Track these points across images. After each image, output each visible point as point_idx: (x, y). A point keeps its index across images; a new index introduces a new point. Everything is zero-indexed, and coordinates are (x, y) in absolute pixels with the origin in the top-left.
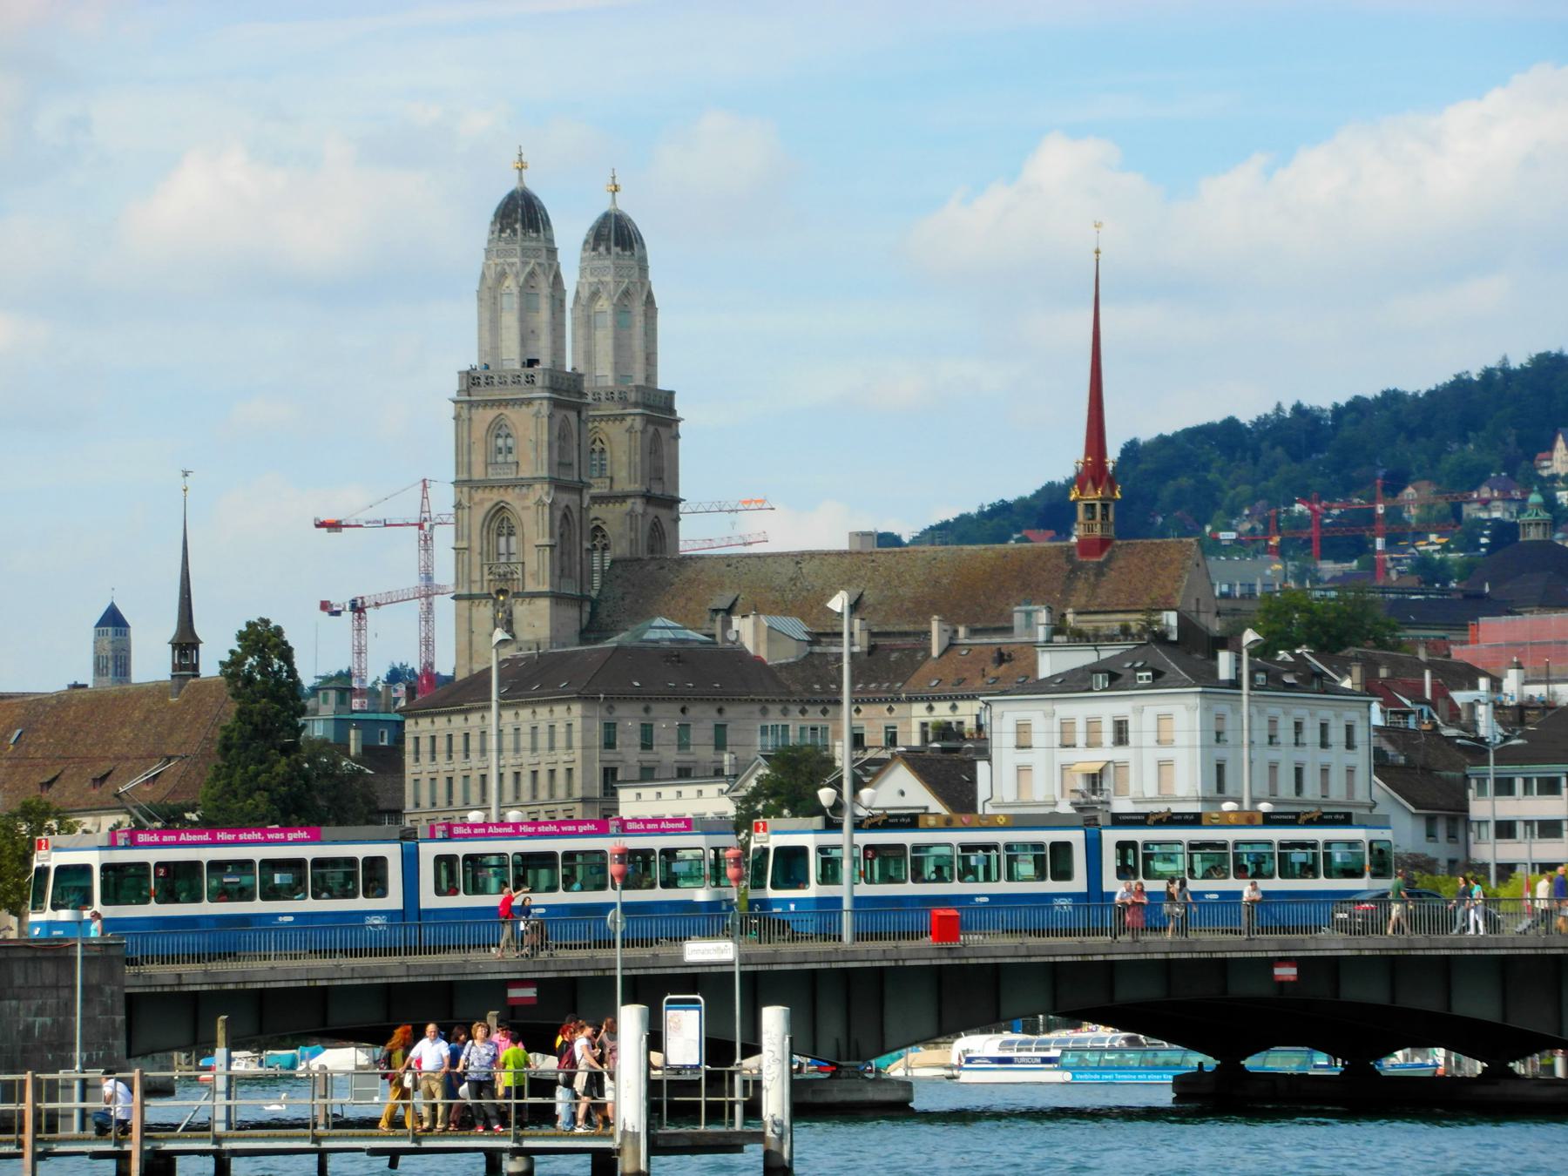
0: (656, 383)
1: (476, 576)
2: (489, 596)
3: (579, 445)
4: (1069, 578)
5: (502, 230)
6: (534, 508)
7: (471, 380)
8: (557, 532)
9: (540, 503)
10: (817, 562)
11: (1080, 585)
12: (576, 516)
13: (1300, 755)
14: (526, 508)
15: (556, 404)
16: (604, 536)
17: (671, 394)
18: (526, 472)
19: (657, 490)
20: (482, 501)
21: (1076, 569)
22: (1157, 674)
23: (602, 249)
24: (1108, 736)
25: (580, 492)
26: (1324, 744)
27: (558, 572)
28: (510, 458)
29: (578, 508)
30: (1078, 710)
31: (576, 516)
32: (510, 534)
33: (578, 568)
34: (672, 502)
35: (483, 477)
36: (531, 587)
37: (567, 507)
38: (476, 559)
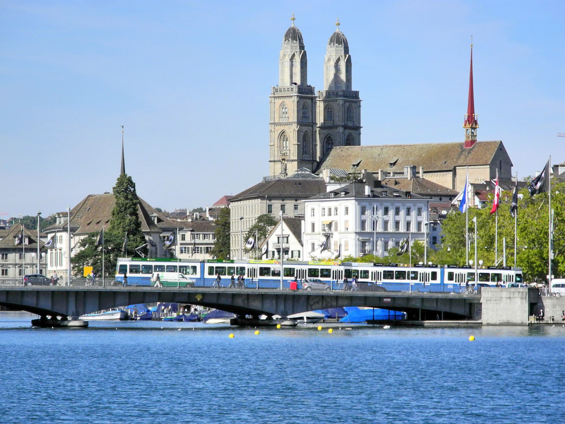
0: (351, 89)
1: (276, 154)
2: (279, 161)
3: (312, 111)
4: (460, 154)
5: (285, 41)
6: (293, 132)
8: (301, 139)
9: (294, 130)
10: (387, 149)
11: (463, 157)
14: (290, 132)
15: (300, 98)
16: (332, 140)
18: (291, 120)
19: (350, 124)
20: (278, 130)
21: (463, 150)
23: (332, 44)
25: (312, 126)
27: (302, 153)
28: (287, 115)
29: (311, 132)
30: (327, 204)
31: (310, 135)
32: (287, 140)
33: (311, 151)
34: (358, 128)
35: (278, 122)
36: (292, 158)
37: (306, 131)
38: (276, 149)
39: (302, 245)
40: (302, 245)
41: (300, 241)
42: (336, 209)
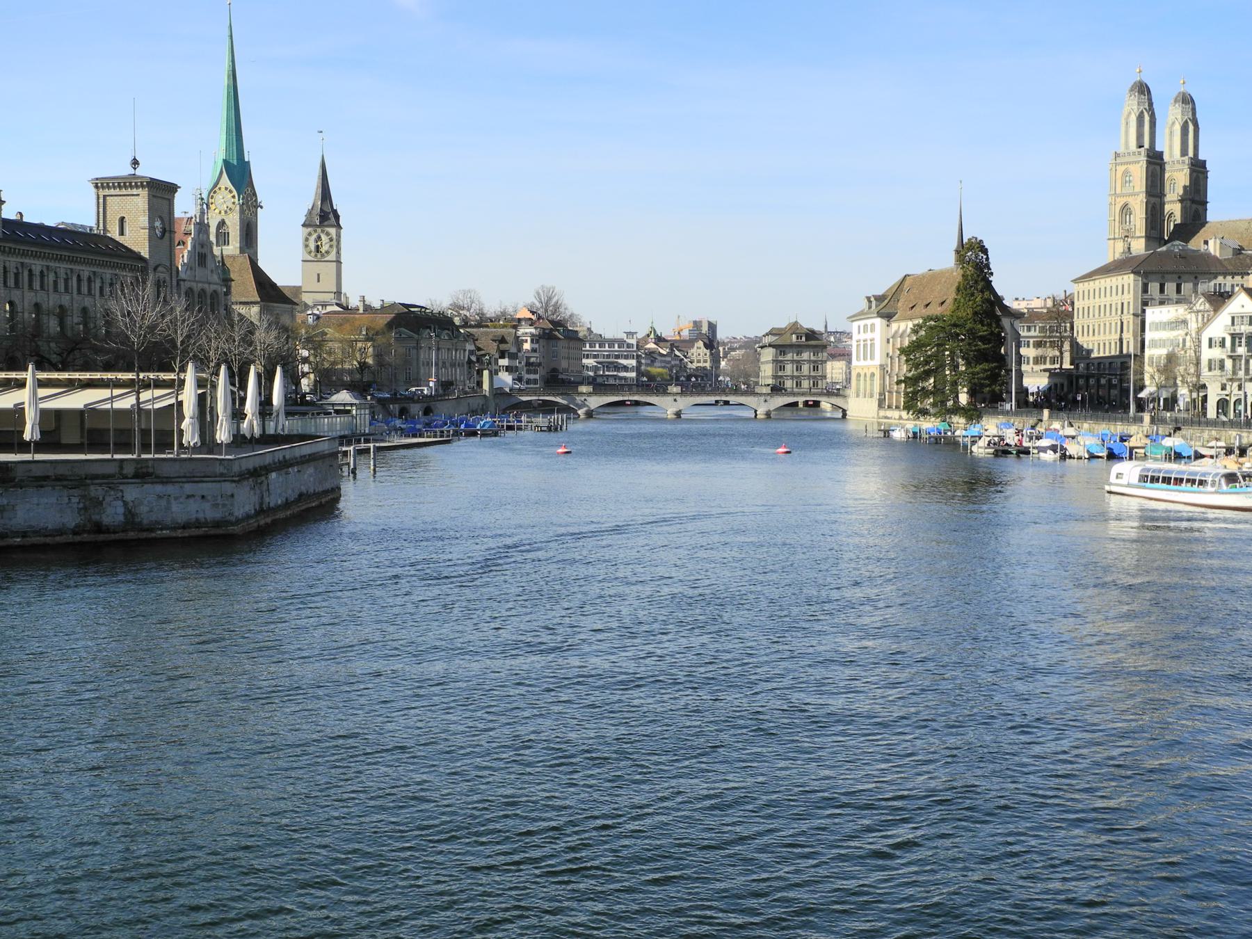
1: (1117, 231)
7: (1117, 155)
9: (1142, 201)
12: (1158, 207)
15: (1149, 163)
17: (1205, 162)
18: (1137, 189)
19: (1197, 198)
31: (1158, 207)
36: (1138, 234)
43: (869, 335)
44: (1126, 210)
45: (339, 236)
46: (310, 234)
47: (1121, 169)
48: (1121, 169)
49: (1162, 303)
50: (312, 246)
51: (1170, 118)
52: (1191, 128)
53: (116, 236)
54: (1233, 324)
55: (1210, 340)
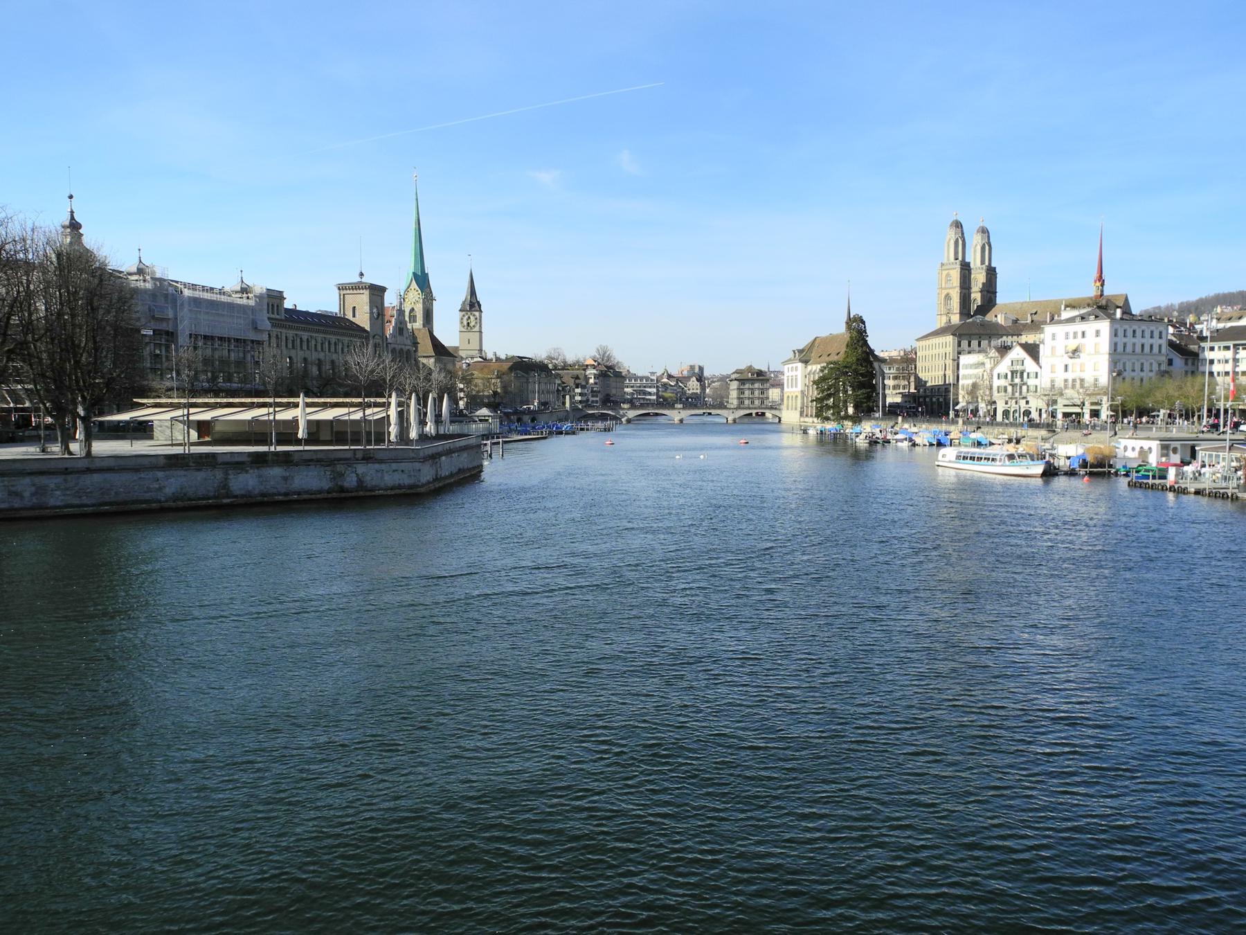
13: (1144, 341)
15: (961, 269)
18: (955, 285)
19: (991, 290)
22: (1096, 317)
24: (1080, 335)
26: (1152, 337)
30: (1071, 328)
39: (1041, 367)
40: (1041, 367)
41: (1038, 363)
42: (1083, 333)
43: (794, 373)
44: (948, 297)
45: (481, 317)
46: (464, 316)
47: (945, 273)
48: (945, 273)
49: (969, 353)
50: (465, 323)
51: (975, 242)
52: (987, 247)
53: (351, 318)
54: (1012, 365)
55: (999, 375)
